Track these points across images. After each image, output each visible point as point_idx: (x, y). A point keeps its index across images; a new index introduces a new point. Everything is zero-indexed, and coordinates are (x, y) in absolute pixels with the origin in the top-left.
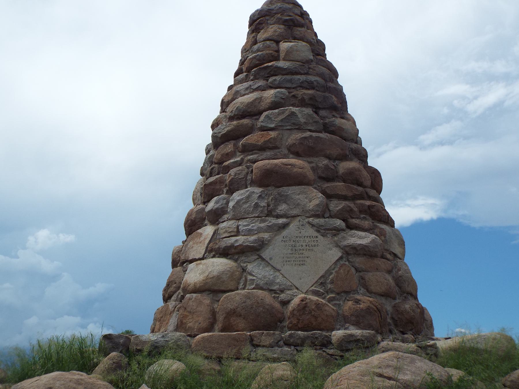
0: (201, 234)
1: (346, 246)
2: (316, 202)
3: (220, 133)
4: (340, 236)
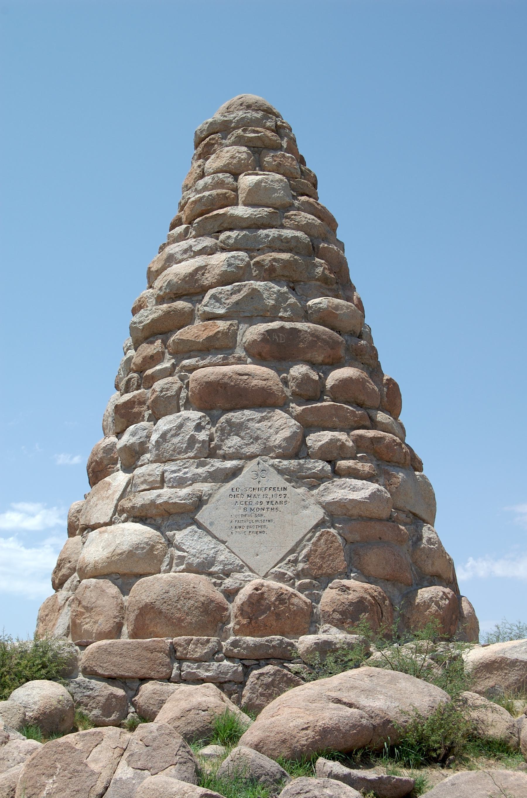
0: (110, 484)
1: (329, 504)
2: (286, 433)
3: (141, 322)
4: (322, 487)
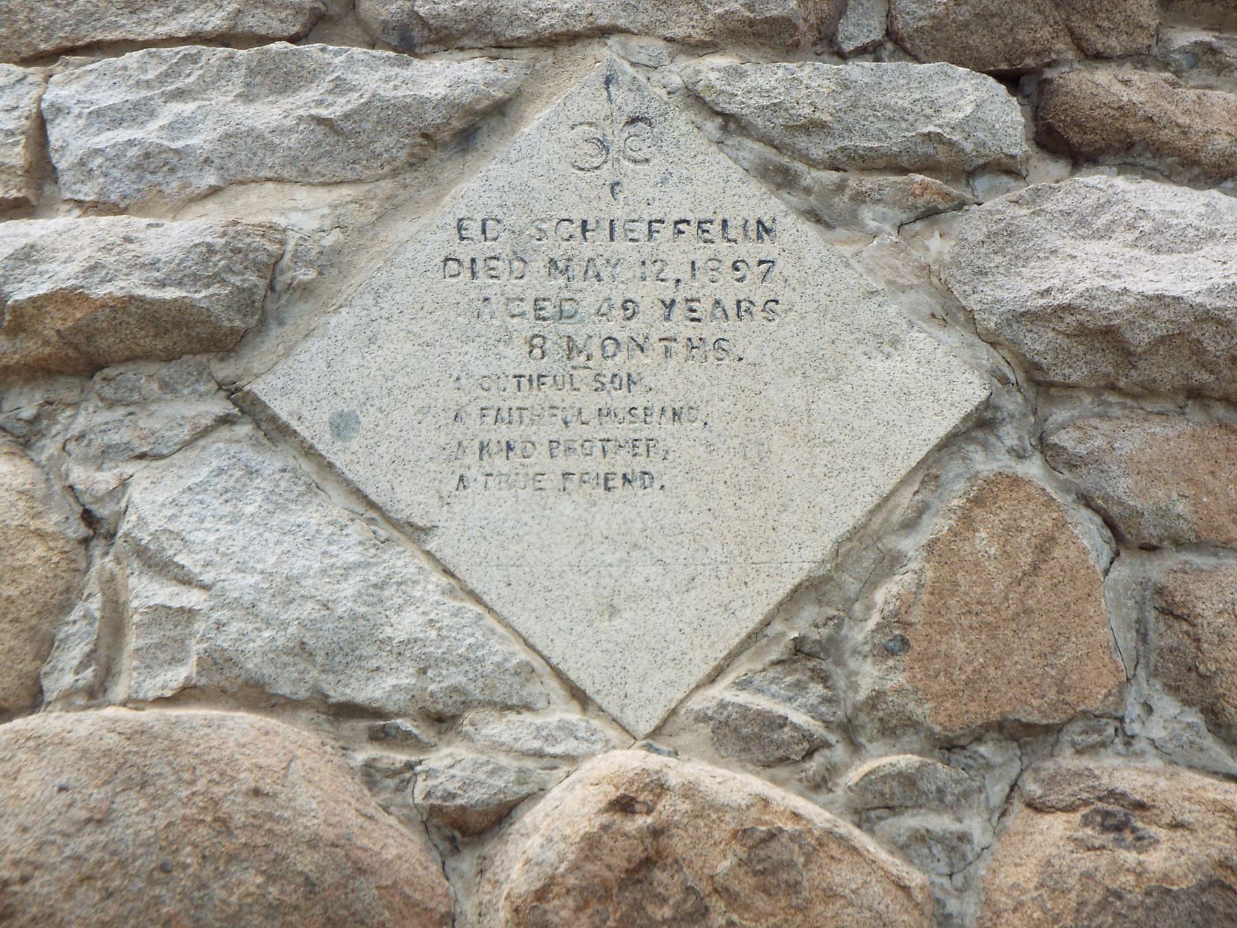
4: (972, 225)
